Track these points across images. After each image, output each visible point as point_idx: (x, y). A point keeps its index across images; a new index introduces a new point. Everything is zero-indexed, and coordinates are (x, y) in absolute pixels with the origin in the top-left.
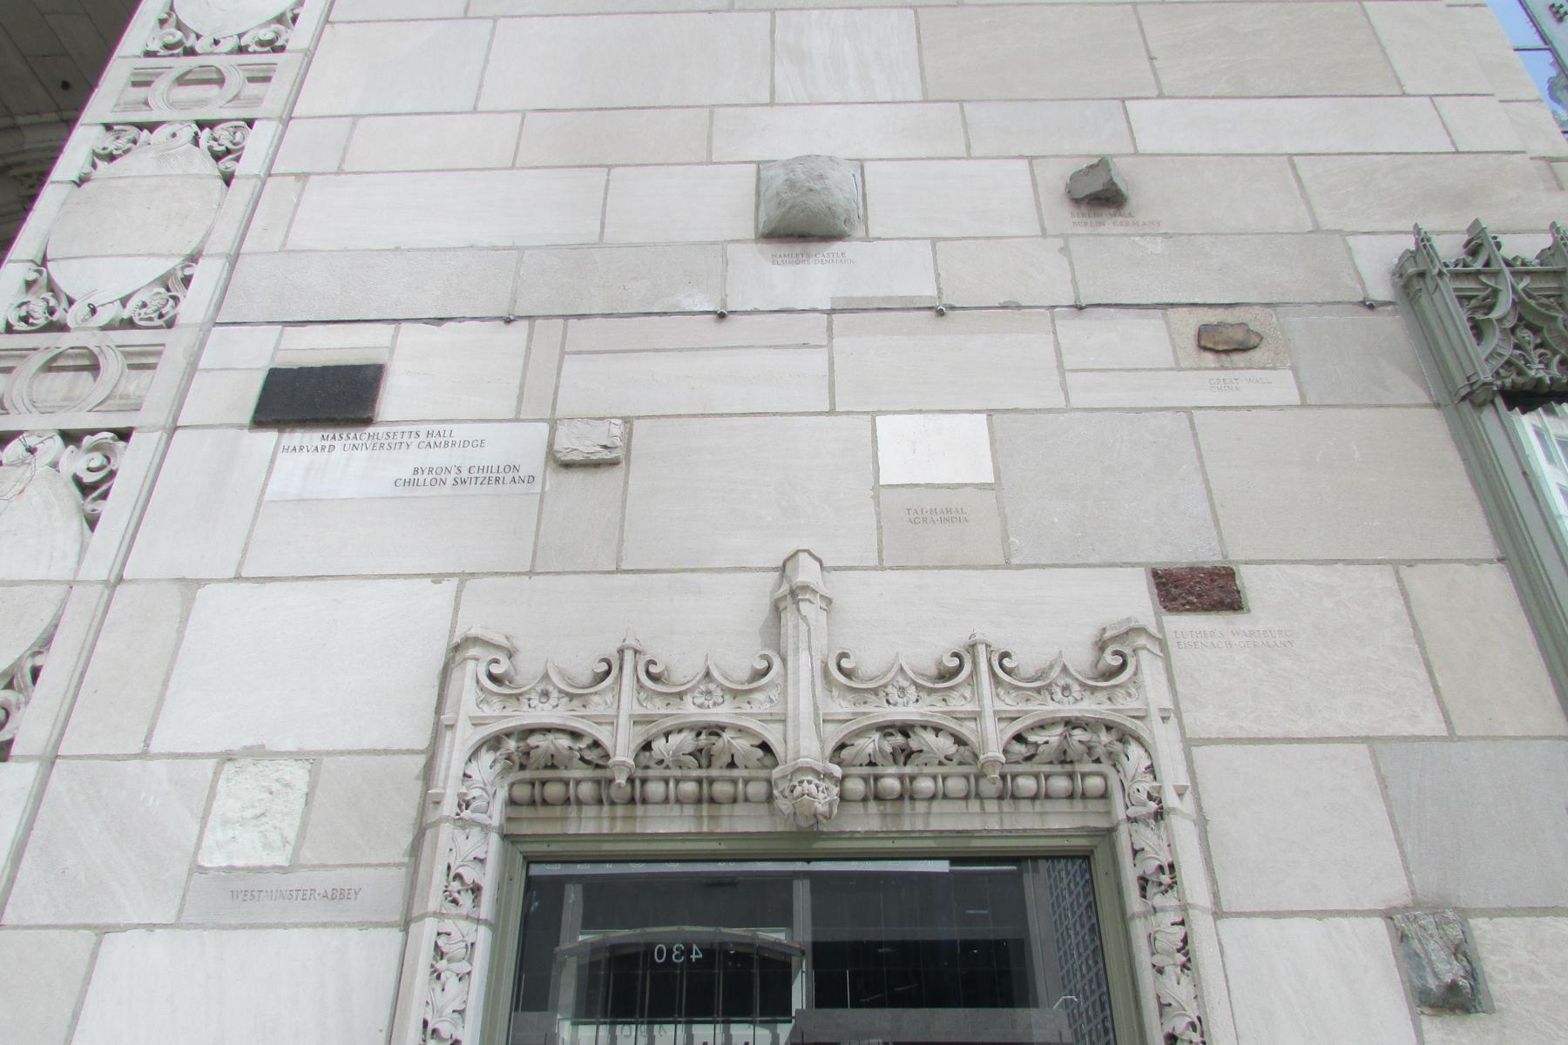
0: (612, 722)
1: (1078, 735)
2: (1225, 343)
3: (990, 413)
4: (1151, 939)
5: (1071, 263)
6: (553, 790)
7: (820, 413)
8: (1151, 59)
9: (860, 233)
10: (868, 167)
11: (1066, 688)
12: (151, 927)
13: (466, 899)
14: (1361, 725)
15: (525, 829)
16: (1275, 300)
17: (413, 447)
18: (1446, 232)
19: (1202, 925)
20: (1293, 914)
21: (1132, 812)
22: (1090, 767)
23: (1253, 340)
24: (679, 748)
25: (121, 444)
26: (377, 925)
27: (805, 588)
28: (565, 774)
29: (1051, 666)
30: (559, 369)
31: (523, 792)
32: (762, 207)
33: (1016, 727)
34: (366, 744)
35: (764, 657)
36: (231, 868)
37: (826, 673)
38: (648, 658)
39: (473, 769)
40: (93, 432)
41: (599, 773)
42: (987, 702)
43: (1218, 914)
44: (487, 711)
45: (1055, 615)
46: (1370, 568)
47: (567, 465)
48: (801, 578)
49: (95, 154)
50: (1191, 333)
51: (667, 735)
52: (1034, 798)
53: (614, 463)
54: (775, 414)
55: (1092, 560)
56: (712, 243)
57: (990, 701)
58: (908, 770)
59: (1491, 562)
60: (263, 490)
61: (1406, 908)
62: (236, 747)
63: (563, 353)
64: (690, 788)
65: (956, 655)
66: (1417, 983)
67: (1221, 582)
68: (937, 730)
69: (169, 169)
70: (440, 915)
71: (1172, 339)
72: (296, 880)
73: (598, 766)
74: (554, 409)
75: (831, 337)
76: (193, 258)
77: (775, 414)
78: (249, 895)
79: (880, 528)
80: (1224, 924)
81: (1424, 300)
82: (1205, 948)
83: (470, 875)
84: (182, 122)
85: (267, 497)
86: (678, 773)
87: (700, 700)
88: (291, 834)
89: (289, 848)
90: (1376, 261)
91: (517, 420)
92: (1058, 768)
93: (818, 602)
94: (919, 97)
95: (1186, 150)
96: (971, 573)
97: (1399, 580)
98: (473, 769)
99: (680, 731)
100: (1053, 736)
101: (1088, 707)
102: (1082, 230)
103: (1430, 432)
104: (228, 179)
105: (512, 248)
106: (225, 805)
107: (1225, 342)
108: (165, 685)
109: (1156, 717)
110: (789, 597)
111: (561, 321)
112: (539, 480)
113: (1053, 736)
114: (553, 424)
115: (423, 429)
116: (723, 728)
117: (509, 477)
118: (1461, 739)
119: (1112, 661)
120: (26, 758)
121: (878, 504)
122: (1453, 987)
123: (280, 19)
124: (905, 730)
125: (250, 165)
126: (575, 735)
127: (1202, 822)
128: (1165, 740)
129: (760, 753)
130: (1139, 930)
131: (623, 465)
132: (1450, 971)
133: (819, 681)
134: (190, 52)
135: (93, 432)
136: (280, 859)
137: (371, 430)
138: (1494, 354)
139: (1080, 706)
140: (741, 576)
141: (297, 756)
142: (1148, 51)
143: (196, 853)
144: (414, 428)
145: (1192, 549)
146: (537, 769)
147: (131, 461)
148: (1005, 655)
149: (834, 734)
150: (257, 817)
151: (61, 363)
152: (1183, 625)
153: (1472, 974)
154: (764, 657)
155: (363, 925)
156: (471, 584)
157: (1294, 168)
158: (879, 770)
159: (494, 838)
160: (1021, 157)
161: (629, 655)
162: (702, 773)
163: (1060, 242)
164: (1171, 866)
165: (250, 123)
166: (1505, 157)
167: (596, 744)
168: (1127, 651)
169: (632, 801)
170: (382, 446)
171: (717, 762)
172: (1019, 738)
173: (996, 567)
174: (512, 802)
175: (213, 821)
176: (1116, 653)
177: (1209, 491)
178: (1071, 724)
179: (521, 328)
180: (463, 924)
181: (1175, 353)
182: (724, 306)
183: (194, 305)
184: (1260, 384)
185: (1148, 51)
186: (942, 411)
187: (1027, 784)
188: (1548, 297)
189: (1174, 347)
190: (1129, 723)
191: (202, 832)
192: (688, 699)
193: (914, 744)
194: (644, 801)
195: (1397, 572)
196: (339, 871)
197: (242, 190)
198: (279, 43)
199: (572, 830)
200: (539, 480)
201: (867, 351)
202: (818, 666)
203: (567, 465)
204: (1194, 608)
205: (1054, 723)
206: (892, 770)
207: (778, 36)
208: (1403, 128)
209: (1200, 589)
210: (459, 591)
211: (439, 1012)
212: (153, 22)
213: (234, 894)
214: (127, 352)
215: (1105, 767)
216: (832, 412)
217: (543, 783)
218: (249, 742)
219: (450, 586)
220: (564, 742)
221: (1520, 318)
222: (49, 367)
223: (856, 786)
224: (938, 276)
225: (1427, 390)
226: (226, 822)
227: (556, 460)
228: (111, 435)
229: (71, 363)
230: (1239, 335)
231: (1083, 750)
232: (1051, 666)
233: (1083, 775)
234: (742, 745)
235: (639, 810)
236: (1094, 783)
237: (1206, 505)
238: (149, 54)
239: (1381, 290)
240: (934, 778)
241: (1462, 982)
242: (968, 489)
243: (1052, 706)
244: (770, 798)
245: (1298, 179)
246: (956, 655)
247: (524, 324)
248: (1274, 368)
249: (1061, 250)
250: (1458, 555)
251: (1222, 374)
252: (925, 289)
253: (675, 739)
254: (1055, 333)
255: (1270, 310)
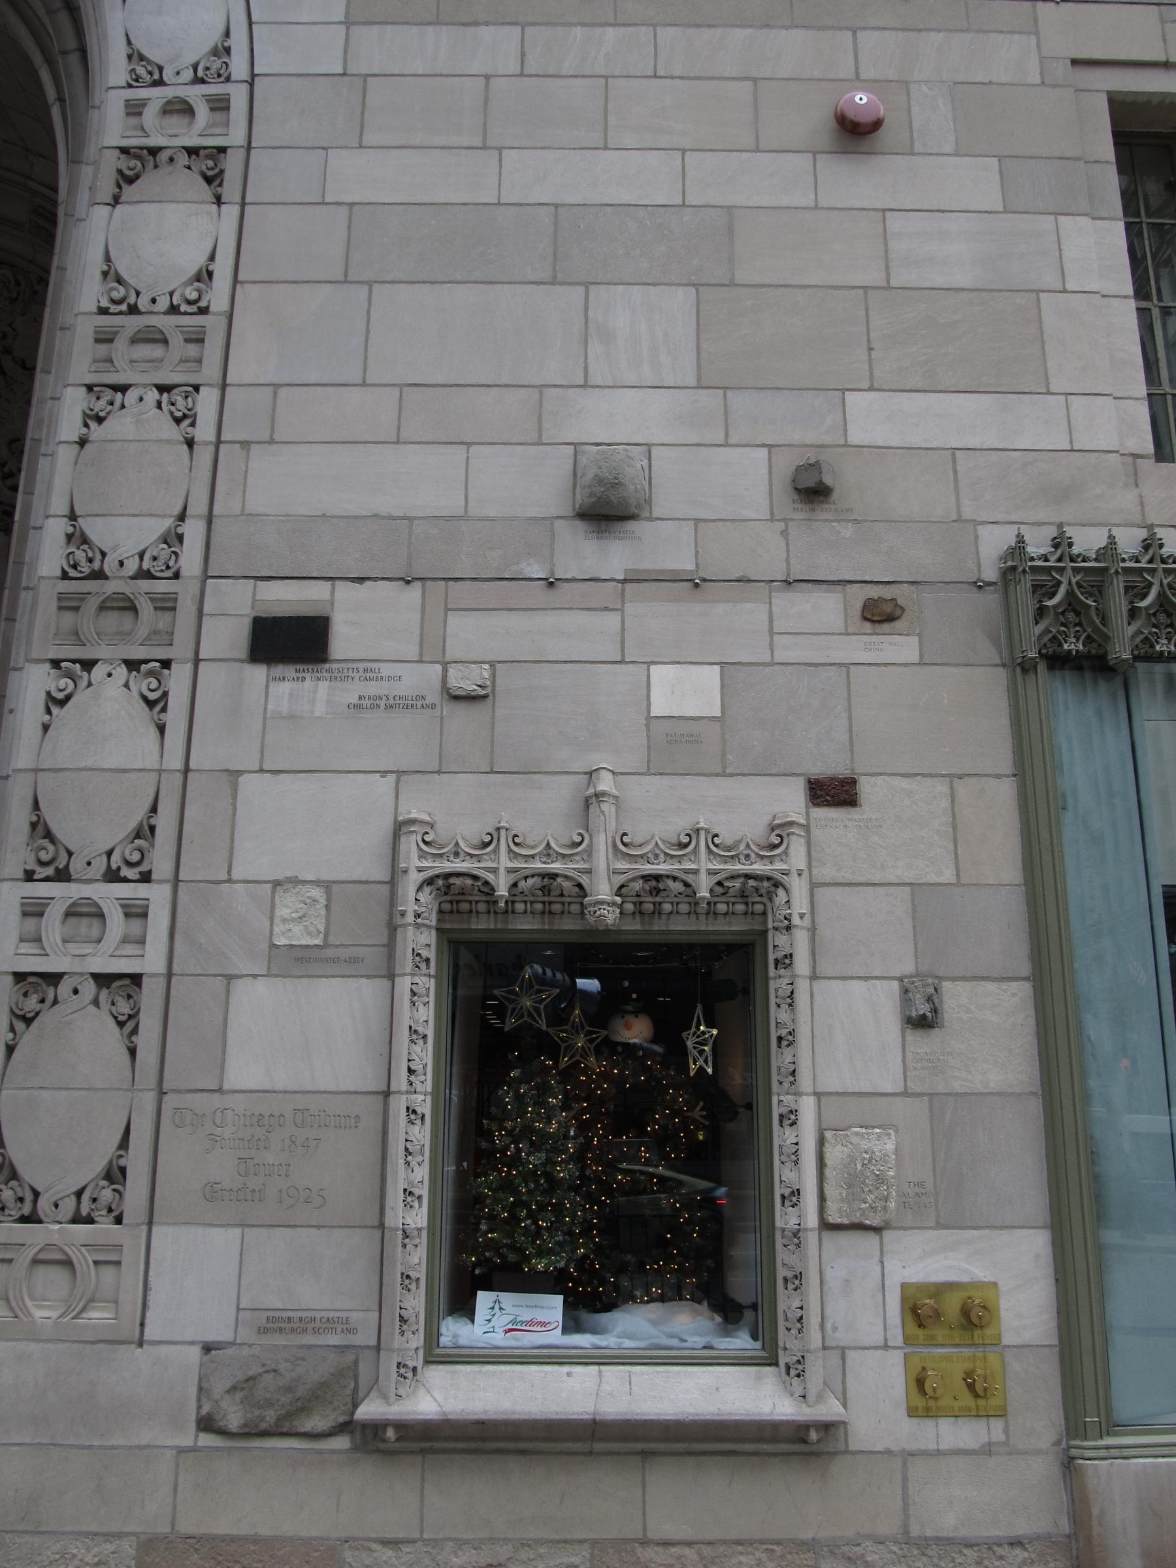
0: (495, 871)
1: (752, 883)
2: (879, 615)
3: (722, 664)
4: (777, 990)
5: (787, 544)
6: (465, 907)
7: (615, 662)
8: (871, 349)
9: (646, 514)
10: (655, 451)
11: (747, 857)
12: (255, 976)
13: (423, 966)
14: (910, 876)
15: (448, 926)
16: (920, 579)
17: (356, 679)
18: (1044, 524)
19: (802, 987)
20: (852, 978)
21: (776, 924)
22: (758, 899)
23: (898, 612)
24: (533, 886)
25: (166, 671)
26: (376, 977)
27: (603, 794)
28: (470, 898)
29: (740, 841)
30: (445, 622)
31: (447, 907)
32: (578, 489)
33: (717, 878)
34: (355, 877)
35: (580, 834)
36: (292, 946)
37: (615, 845)
38: (514, 833)
39: (421, 896)
40: (146, 662)
41: (488, 898)
42: (703, 864)
43: (814, 977)
44: (425, 864)
45: (748, 808)
46: (936, 779)
47: (456, 698)
48: (601, 787)
49: (84, 414)
50: (859, 605)
51: (526, 878)
52: (726, 914)
53: (485, 697)
54: (586, 662)
55: (774, 771)
56: (543, 518)
57: (705, 863)
58: (658, 899)
59: (1008, 776)
60: (265, 709)
61: (911, 976)
62: (280, 877)
63: (447, 610)
64: (539, 906)
65: (688, 835)
66: (908, 1013)
67: (847, 788)
68: (675, 879)
69: (140, 423)
70: (413, 975)
71: (845, 610)
72: (329, 952)
73: (487, 894)
74: (444, 654)
75: (623, 603)
76: (182, 517)
77: (586, 662)
78: (308, 960)
79: (649, 747)
80: (816, 984)
81: (1012, 588)
82: (802, 998)
83: (425, 953)
84: (145, 386)
85: (269, 715)
86: (532, 899)
87: (544, 859)
88: (322, 928)
89: (322, 936)
90: (993, 544)
91: (420, 661)
92: (740, 900)
93: (612, 801)
94: (694, 384)
95: (880, 443)
96: (702, 778)
97: (952, 788)
98: (421, 896)
99: (533, 876)
100: (737, 884)
101: (758, 867)
102: (801, 515)
103: (987, 688)
104: (190, 443)
105: (404, 518)
106: (282, 912)
107: (880, 615)
108: (232, 840)
109: (794, 874)
110: (590, 801)
111: (443, 583)
112: (438, 707)
113: (737, 884)
114: (445, 665)
115: (361, 666)
116: (557, 875)
117: (419, 704)
118: (963, 885)
119: (779, 835)
120: (161, 882)
121: (648, 730)
122: (924, 1017)
123: (198, 278)
124: (658, 878)
125: (204, 431)
126: (475, 878)
127: (813, 930)
128: (799, 889)
129: (577, 889)
130: (772, 985)
131: (491, 697)
132: (924, 1009)
133: (610, 850)
134: (133, 310)
135: (146, 662)
136: (318, 941)
137: (327, 666)
138: (1047, 631)
139: (755, 866)
140: (565, 777)
141: (316, 883)
142: (869, 341)
143: (271, 937)
144: (355, 665)
145: (832, 765)
146: (456, 895)
147: (177, 681)
148: (716, 835)
149: (619, 880)
150: (300, 918)
151: (109, 604)
152: (820, 813)
153: (935, 1011)
154: (580, 834)
155: (368, 977)
156: (404, 778)
157: (954, 461)
158: (642, 899)
159: (434, 932)
160: (763, 445)
161: (503, 832)
162: (546, 899)
163: (782, 525)
164: (791, 955)
165: (197, 388)
166: (1104, 456)
167: (487, 883)
168: (784, 834)
169: (506, 912)
170: (336, 678)
171: (553, 893)
172: (719, 883)
173: (717, 775)
174: (440, 912)
175: (277, 920)
176: (778, 835)
177: (851, 725)
178: (748, 876)
179: (416, 590)
180: (423, 978)
181: (846, 621)
182: (552, 573)
183: (190, 559)
184: (898, 647)
185: (869, 341)
186: (692, 663)
187: (722, 908)
188: (1092, 586)
189: (846, 616)
190: (778, 876)
191: (272, 925)
192: (537, 858)
193: (661, 886)
194: (513, 912)
195: (951, 782)
196: (352, 948)
197: (204, 456)
198: (203, 304)
199: (474, 927)
200: (438, 707)
201: (650, 614)
202: (610, 840)
203: (456, 698)
204: (829, 804)
205: (739, 876)
206: (651, 899)
207: (591, 314)
208: (1035, 426)
209: (832, 792)
210: (397, 783)
211: (416, 1021)
212: (98, 277)
213: (297, 960)
214: (153, 598)
215: (765, 900)
216: (622, 662)
217: (458, 902)
218: (288, 874)
219: (392, 778)
220: (469, 882)
221: (1070, 605)
222: (102, 608)
223: (629, 907)
224: (697, 552)
225: (1000, 653)
226: (284, 920)
227: (449, 694)
228: (158, 664)
229: (115, 605)
230: (888, 608)
231: (757, 892)
232: (740, 841)
233: (753, 903)
234: (567, 884)
235: (511, 916)
236: (759, 908)
237: (847, 735)
238: (103, 311)
239: (990, 573)
240: (672, 903)
241: (929, 1015)
242: (704, 721)
243: (739, 867)
244: (582, 913)
245: (955, 472)
246: (688, 835)
247: (418, 584)
248: (907, 635)
249: (782, 532)
250: (990, 771)
251: (874, 638)
252: (687, 564)
253: (530, 881)
254: (770, 603)
255: (913, 588)
